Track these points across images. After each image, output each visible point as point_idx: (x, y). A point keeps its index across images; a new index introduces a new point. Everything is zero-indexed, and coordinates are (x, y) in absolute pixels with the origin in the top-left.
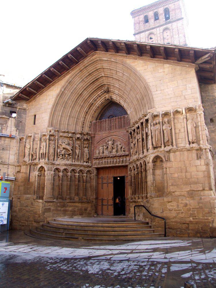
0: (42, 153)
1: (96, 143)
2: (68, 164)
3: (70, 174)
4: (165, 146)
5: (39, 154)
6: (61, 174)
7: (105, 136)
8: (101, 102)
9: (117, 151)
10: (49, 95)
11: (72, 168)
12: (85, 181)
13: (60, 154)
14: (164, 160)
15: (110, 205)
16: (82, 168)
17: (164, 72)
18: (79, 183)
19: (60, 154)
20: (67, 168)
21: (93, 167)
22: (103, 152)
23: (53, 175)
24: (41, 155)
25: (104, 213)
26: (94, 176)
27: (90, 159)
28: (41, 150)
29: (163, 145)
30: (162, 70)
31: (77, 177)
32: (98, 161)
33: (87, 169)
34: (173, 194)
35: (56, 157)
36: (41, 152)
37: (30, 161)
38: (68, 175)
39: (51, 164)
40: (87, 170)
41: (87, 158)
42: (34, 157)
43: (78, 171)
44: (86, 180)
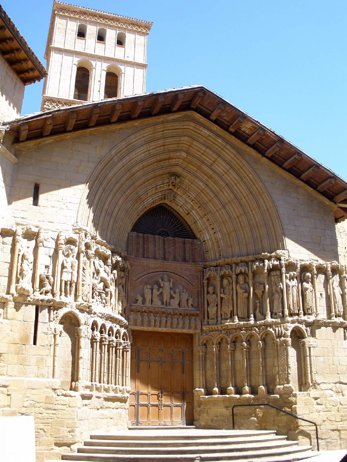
0: (66, 283)
1: (134, 279)
2: (107, 315)
4: (304, 315)
5: (61, 281)
7: (152, 268)
8: (154, 200)
9: (179, 304)
10: (79, 151)
14: (306, 336)
15: (153, 405)
17: (298, 199)
22: (152, 301)
24: (63, 285)
25: (140, 420)
28: (64, 274)
29: (301, 311)
30: (294, 195)
34: (318, 386)
36: (66, 277)
37: (37, 293)
38: (104, 339)
42: (48, 287)
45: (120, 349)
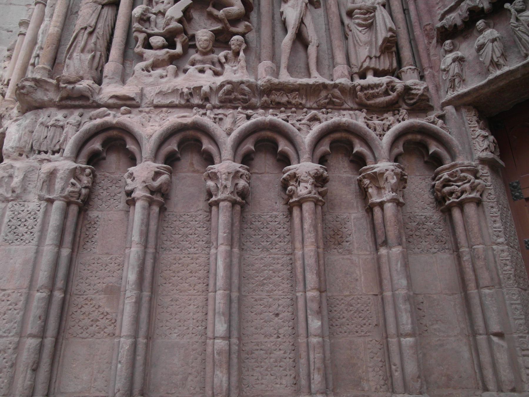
3: (237, 166)
6: (144, 170)
11: (253, 120)
12: (392, 232)
13: (149, 35)
16: (345, 117)
18: (336, 257)
19: (149, 35)
20: (207, 121)
21: (451, 95)
23: (58, 184)
26: (475, 173)
27: (406, 53)
31: (303, 190)
32: (490, 33)
33: (398, 123)
35: (115, 52)
39: (60, 107)
40: (397, 127)
41: (382, 34)
43: (306, 138)
44: (402, 224)
45: (381, 205)
